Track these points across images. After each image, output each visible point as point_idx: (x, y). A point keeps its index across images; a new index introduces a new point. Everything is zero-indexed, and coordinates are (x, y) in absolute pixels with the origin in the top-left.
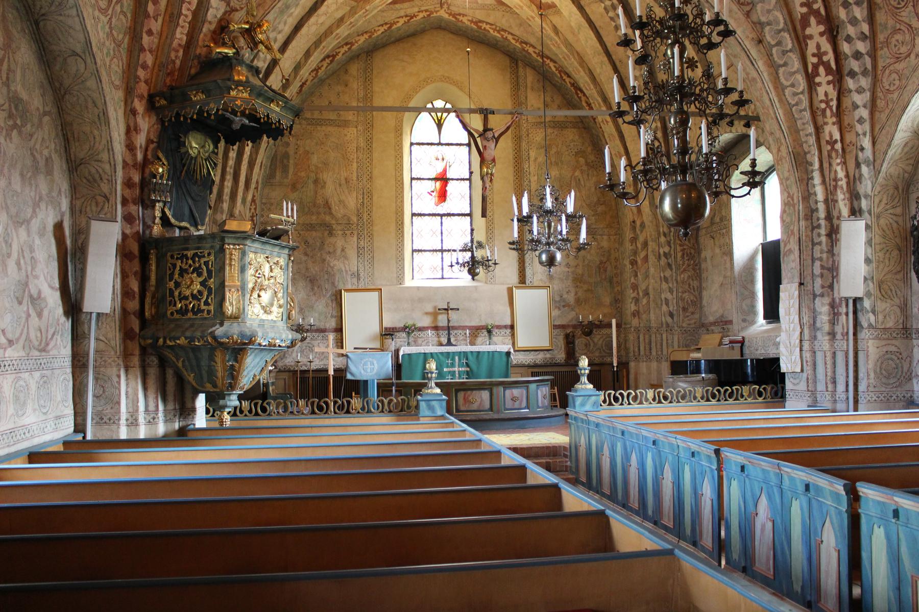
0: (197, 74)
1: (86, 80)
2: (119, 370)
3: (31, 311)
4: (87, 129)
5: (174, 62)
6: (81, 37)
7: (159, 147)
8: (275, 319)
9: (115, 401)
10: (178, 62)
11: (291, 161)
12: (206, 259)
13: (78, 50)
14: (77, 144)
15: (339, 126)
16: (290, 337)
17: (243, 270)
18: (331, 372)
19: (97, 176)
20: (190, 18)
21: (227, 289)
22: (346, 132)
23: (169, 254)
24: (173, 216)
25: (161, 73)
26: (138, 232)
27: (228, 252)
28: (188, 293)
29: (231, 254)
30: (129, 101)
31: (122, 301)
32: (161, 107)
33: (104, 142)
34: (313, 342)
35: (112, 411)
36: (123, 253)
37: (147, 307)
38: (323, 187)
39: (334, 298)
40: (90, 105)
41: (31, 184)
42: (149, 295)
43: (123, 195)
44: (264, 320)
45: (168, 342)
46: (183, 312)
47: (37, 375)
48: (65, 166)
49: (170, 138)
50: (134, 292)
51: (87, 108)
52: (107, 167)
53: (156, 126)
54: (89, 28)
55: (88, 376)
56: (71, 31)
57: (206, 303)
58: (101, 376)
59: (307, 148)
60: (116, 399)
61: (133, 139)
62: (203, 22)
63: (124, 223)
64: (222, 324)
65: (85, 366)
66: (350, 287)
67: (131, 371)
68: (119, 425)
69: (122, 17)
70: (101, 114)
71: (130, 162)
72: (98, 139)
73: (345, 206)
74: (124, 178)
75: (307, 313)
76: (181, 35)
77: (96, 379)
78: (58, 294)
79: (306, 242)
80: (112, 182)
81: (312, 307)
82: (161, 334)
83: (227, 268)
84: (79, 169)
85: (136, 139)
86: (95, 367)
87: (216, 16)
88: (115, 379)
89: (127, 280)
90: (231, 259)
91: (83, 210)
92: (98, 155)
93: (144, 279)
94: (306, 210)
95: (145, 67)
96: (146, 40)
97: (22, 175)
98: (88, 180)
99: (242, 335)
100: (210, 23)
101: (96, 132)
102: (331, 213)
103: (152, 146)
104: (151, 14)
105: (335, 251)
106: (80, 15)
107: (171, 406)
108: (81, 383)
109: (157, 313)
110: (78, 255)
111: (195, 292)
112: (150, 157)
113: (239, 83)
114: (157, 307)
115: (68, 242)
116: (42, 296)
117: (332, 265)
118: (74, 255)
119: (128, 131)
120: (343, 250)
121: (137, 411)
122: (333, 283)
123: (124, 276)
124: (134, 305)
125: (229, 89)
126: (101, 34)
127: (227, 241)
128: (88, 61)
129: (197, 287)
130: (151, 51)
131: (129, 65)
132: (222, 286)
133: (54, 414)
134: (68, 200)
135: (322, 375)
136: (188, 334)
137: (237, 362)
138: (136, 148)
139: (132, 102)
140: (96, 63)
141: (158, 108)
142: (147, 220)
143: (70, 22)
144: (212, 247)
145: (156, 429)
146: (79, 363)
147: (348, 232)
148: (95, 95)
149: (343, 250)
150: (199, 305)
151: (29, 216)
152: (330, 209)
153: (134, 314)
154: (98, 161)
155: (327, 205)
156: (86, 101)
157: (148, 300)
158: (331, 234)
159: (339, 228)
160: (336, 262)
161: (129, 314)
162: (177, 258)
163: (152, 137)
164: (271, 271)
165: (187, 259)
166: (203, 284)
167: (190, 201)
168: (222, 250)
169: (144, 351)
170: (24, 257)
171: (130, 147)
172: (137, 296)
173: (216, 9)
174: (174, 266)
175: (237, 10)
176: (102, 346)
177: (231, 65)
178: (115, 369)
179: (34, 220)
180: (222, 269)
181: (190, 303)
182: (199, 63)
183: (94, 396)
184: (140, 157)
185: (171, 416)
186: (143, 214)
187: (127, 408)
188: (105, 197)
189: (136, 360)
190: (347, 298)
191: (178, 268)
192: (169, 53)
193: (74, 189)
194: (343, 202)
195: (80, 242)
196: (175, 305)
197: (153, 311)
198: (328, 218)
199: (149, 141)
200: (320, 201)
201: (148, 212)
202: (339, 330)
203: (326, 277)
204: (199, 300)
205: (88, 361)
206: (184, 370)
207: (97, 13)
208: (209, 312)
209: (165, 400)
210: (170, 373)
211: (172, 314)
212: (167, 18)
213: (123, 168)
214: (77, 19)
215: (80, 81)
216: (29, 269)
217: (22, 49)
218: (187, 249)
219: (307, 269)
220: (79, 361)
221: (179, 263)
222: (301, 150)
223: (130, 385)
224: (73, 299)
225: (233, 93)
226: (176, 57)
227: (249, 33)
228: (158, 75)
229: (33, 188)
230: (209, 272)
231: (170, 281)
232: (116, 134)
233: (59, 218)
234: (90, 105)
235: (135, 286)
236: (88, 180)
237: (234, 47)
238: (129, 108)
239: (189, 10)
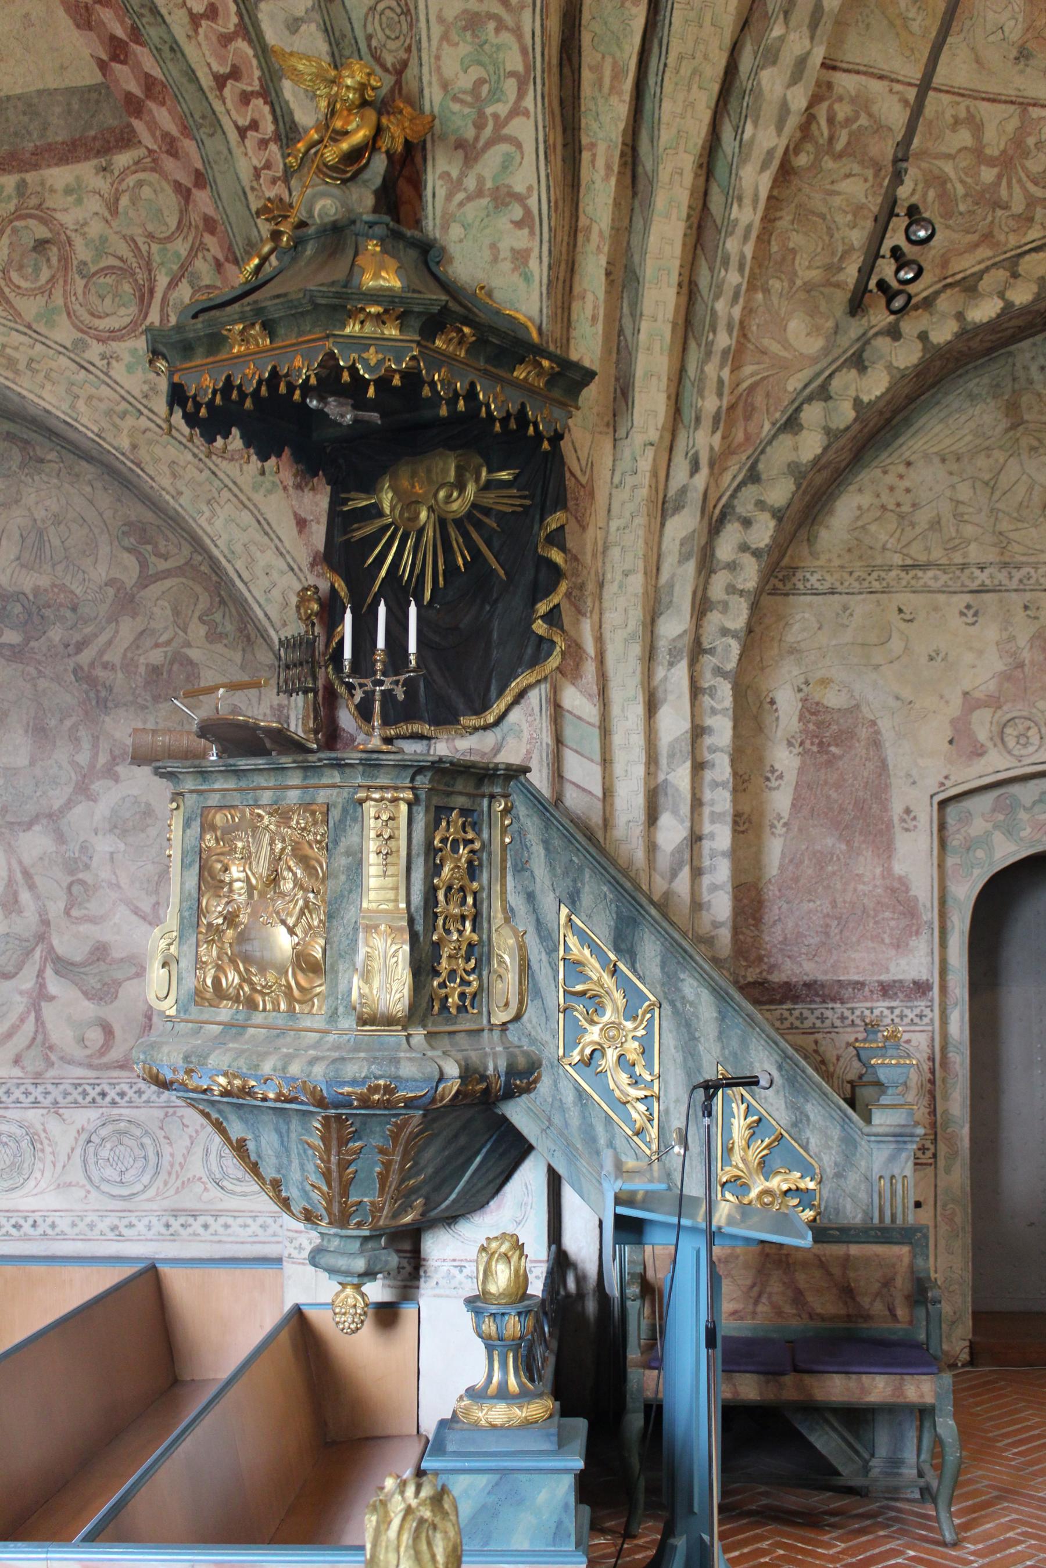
3: (54, 985)
41: (75, 741)
47: (87, 1117)
97: (40, 732)
116: (116, 954)
133: (166, 1204)
151: (57, 805)
170: (32, 887)
179: (79, 810)
207: (94, 351)
216: (56, 908)
217: (30, 497)
229: (86, 745)
232: (267, 558)
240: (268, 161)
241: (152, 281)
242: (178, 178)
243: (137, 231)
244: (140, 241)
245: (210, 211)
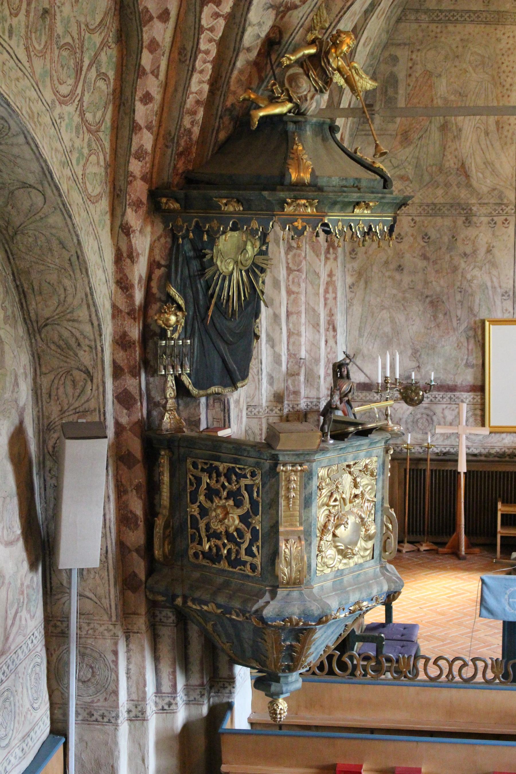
0: (228, 140)
1: (46, 216)
2: (116, 644)
4: (53, 278)
5: (189, 132)
6: (35, 166)
7: (167, 278)
8: (361, 561)
9: (110, 689)
10: (196, 130)
11: (401, 91)
12: (248, 482)
13: (31, 180)
14: (38, 298)
15: (486, 23)
16: (385, 588)
17: (307, 502)
18: (462, 467)
19: (74, 345)
20: (214, 53)
21: (281, 538)
22: (499, 35)
23: (189, 461)
24: (195, 385)
25: (169, 151)
26: (140, 422)
27: (283, 476)
28: (221, 529)
29: (289, 481)
30: (119, 212)
31: (119, 532)
32: (170, 211)
33: (80, 295)
34: (434, 407)
35: (106, 704)
36: (120, 458)
37: (157, 542)
38: (457, 137)
39: (471, 333)
40: (55, 245)
42: (160, 522)
43: (114, 362)
44: (340, 573)
45: (190, 604)
46: (214, 557)
48: (21, 330)
49: (186, 260)
50: (136, 516)
51: (51, 250)
52: (87, 329)
53: (163, 240)
54: (46, 153)
55: (68, 651)
56: (18, 161)
57: (249, 552)
58: (88, 651)
59: (430, 66)
60: (112, 686)
61: (127, 271)
62: (237, 52)
63: (118, 406)
64: (274, 595)
65: (64, 635)
66: (499, 315)
67: (134, 638)
68: (117, 725)
69: (101, 84)
70: (74, 259)
71: (123, 306)
72: (70, 290)
73: (494, 172)
74: (115, 332)
75: (424, 356)
76: (199, 85)
77: (82, 655)
78: (21, 544)
79: (426, 237)
80: (95, 349)
81: (433, 348)
82: (179, 591)
83: (282, 502)
84: (44, 331)
85: (132, 271)
86: (79, 637)
87: (259, 36)
88: (110, 657)
89: (124, 498)
90: (288, 489)
91: (54, 393)
92: (72, 312)
93: (152, 489)
94: (427, 178)
95: (140, 155)
96: (142, 113)
98: (59, 347)
99: (306, 615)
100: (249, 50)
101: (67, 282)
102: (469, 185)
103: (158, 273)
104: (148, 68)
105: (475, 251)
106: (30, 142)
107: (195, 680)
108: (59, 660)
109: (172, 551)
110: (49, 464)
111: (231, 530)
112: (155, 290)
113: (299, 189)
114: (172, 543)
115: (33, 448)
117: (469, 277)
118: (42, 464)
119: (118, 259)
120: (489, 251)
121: (144, 699)
122: (471, 309)
123: (120, 491)
124: (136, 537)
125: (282, 203)
126: (66, 137)
127: (281, 458)
128: (49, 192)
129: (234, 521)
130: (149, 128)
131: (115, 151)
132: (273, 532)
134: (30, 380)
135: (449, 467)
136: (221, 600)
137: (298, 641)
138: (132, 286)
139: (123, 214)
140: (60, 195)
141: (164, 211)
142: (153, 393)
143: (15, 151)
144: (258, 465)
145: (173, 721)
146: (55, 630)
147: (499, 220)
148: (64, 235)
149: (489, 251)
150: (238, 553)
152: (467, 176)
153: (137, 551)
154: (73, 321)
155: (463, 170)
156: (48, 241)
157: (158, 531)
158: (468, 221)
159: (483, 210)
160: (476, 272)
161: (130, 551)
162: (203, 470)
163: (158, 258)
164: (356, 486)
165: (219, 475)
166: (243, 519)
167: (222, 346)
168: (273, 473)
169: (153, 606)
171: (123, 284)
172: (141, 524)
173: (259, 23)
174: (199, 480)
175: (296, 7)
176: (89, 606)
177: (286, 132)
178: (109, 643)
180: (274, 503)
181: (224, 545)
182: (232, 119)
183: (78, 679)
184: (139, 296)
185: (195, 695)
186: (147, 384)
187: (129, 694)
188: (87, 372)
189: (141, 623)
190: (494, 334)
191: (204, 486)
192: (181, 118)
193: (37, 359)
194: (492, 164)
195: (51, 443)
196: (200, 543)
197: (167, 548)
198: (463, 194)
199: (153, 265)
200: (450, 163)
201: (155, 381)
202: (480, 389)
203: (458, 297)
204: (239, 545)
205: (68, 627)
206: (217, 638)
208: (253, 568)
209: (187, 671)
210: (194, 632)
211: (196, 555)
212: (175, 55)
213: (114, 317)
214: (26, 148)
215: (37, 217)
218: (218, 459)
219: (426, 283)
220: (55, 626)
221: (206, 479)
222: (419, 70)
223: (133, 660)
224: (43, 533)
225: (289, 209)
226: (192, 123)
227: (317, 63)
228: (164, 154)
230: (254, 503)
231: (193, 501)
232: (100, 273)
233: (17, 422)
234: (55, 245)
235: (137, 507)
236: (59, 347)
237: (290, 100)
238: (118, 223)
239: (210, 41)
240: (213, 26)
241: (82, 61)
242: (149, 7)
243: (82, 19)
244: (83, 26)
245: (159, 39)
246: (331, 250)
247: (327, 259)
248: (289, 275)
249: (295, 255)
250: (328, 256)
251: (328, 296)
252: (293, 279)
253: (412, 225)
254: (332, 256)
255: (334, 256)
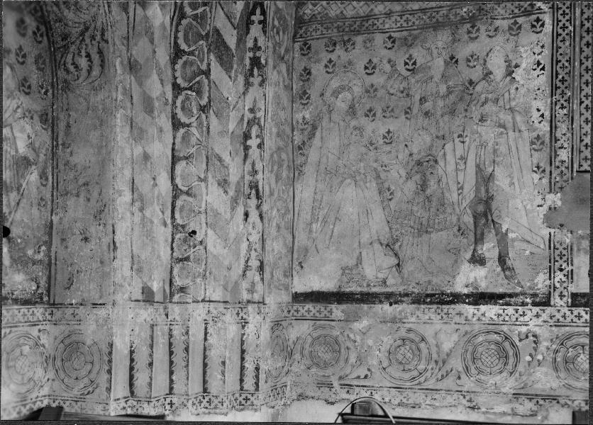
246: (256, 70)
247: (248, 84)
248: (175, 97)
249: (185, 63)
250: (251, 79)
251: (249, 142)
252: (183, 102)
253: (390, 45)
254: (256, 80)
255: (260, 78)
